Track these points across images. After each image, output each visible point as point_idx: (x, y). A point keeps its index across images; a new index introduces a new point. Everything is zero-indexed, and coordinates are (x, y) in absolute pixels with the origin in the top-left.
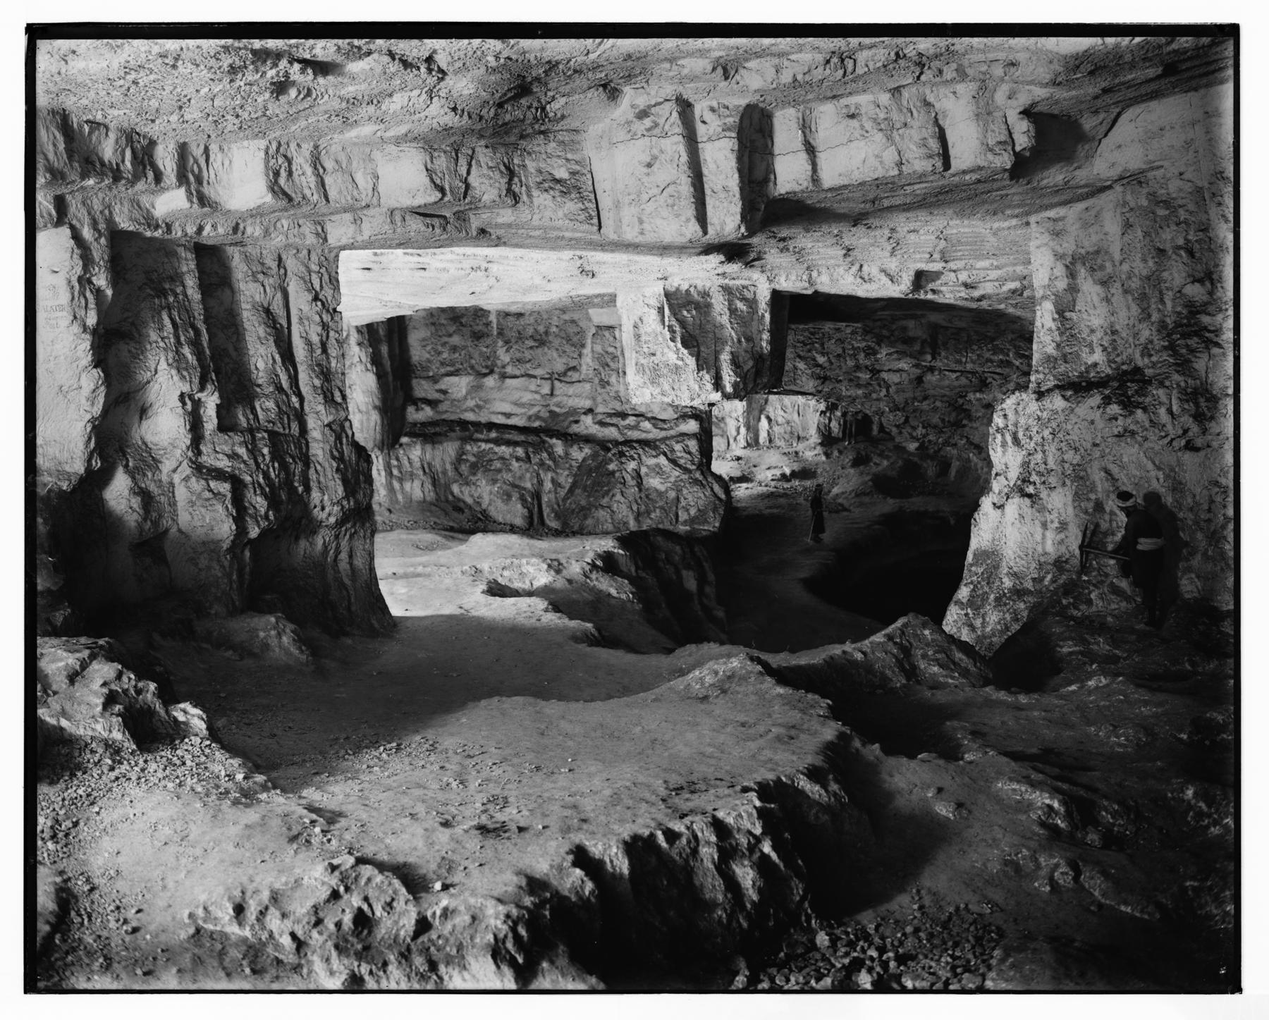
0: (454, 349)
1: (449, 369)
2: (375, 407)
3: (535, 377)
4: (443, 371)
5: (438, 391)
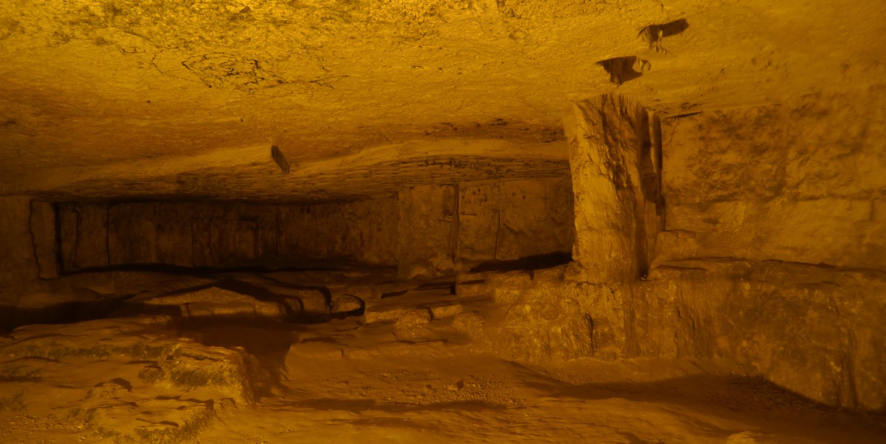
0: (728, 169)
1: (720, 193)
2: (614, 226)
3: (843, 197)
4: (713, 195)
5: (708, 221)
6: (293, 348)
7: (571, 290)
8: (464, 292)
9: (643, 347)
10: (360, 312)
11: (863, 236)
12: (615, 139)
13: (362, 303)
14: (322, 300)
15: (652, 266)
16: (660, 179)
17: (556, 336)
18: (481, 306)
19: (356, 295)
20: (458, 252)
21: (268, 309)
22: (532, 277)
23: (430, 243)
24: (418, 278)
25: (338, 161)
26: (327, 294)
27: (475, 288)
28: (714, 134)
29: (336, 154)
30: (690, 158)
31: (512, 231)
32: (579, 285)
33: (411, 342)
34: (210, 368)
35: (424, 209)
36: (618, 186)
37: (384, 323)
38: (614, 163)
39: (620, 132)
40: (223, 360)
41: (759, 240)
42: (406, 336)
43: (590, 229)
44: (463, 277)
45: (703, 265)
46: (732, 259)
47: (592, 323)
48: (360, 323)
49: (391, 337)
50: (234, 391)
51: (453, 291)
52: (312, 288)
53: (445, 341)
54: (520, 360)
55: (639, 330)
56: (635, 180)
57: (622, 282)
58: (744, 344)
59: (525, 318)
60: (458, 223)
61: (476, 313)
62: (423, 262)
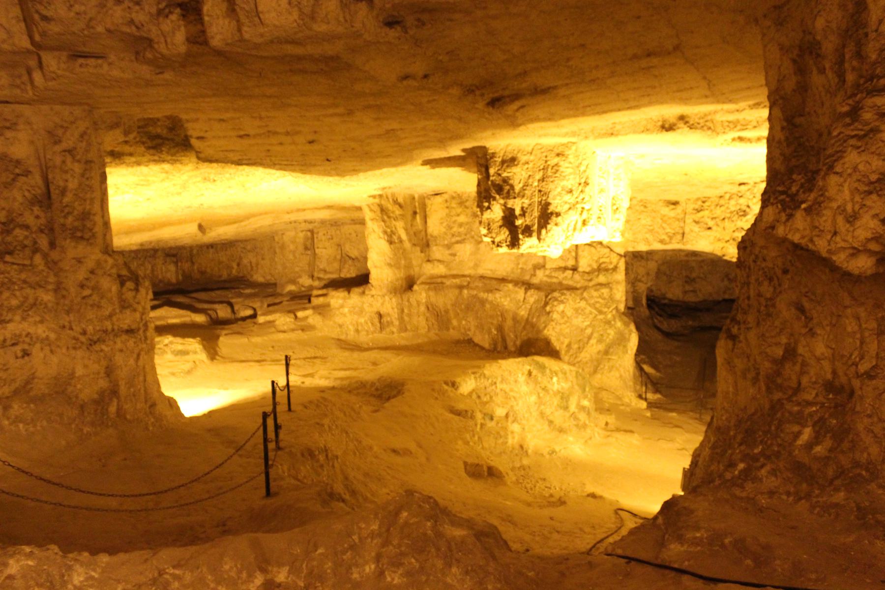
2: (390, 265)
4: (454, 240)
5: (451, 255)
6: (221, 339)
7: (367, 299)
8: (315, 301)
9: (409, 328)
10: (254, 316)
11: (518, 264)
12: (389, 217)
13: (255, 310)
14: (229, 310)
15: (418, 282)
16: (426, 231)
17: (361, 324)
18: (323, 310)
19: (251, 304)
20: (316, 275)
21: (200, 318)
22: (349, 292)
23: (297, 269)
24: (290, 292)
25: (236, 226)
26: (231, 305)
27: (321, 299)
28: (454, 205)
29: (235, 222)
30: (442, 219)
31: (350, 258)
32: (373, 296)
33: (284, 332)
34: (189, 348)
35: (292, 247)
36: (391, 242)
37: (270, 322)
38: (389, 230)
39: (393, 212)
40: (194, 345)
41: (476, 266)
42: (282, 328)
43: (376, 267)
44: (315, 292)
45: (444, 280)
46: (464, 276)
47: (380, 316)
48: (255, 323)
49: (273, 330)
50: (203, 356)
51: (310, 301)
52: (221, 302)
53: (303, 330)
54: (343, 337)
55: (406, 318)
56: (404, 237)
57: (395, 293)
58: (464, 322)
59: (345, 315)
60: (315, 254)
61: (320, 314)
62: (293, 282)
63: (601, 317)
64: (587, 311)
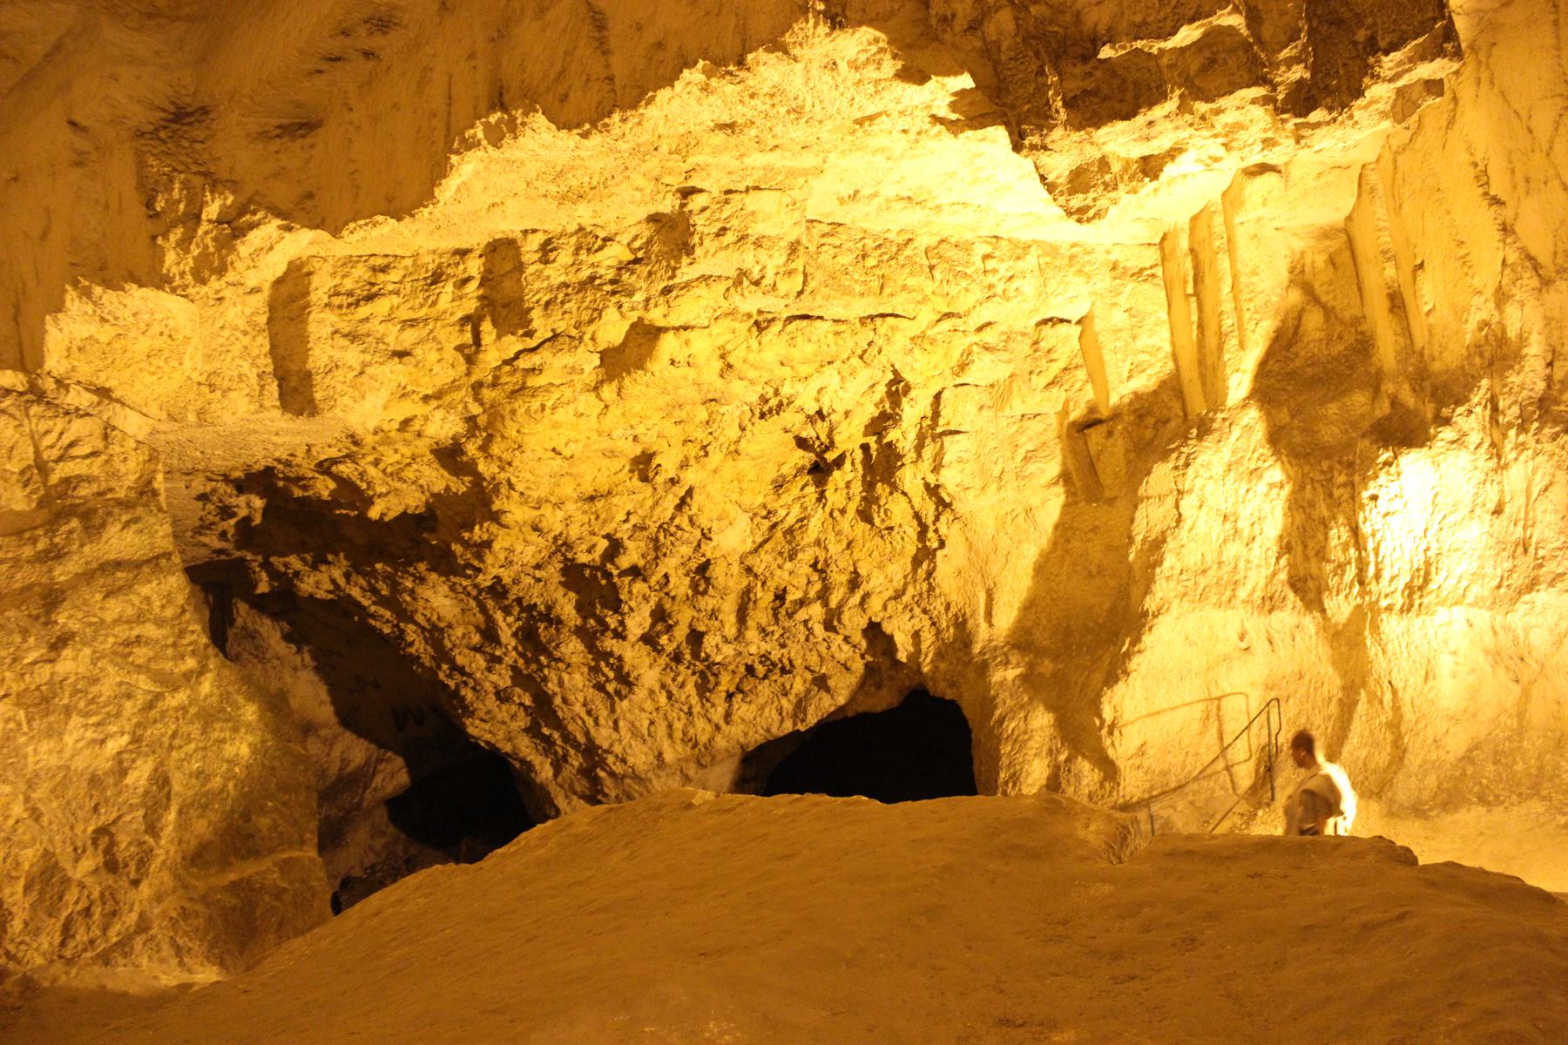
63: (182, 697)
64: (106, 689)
